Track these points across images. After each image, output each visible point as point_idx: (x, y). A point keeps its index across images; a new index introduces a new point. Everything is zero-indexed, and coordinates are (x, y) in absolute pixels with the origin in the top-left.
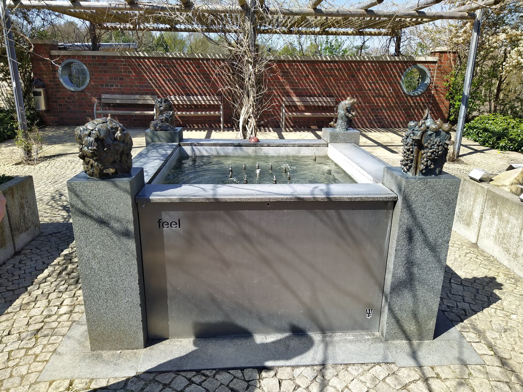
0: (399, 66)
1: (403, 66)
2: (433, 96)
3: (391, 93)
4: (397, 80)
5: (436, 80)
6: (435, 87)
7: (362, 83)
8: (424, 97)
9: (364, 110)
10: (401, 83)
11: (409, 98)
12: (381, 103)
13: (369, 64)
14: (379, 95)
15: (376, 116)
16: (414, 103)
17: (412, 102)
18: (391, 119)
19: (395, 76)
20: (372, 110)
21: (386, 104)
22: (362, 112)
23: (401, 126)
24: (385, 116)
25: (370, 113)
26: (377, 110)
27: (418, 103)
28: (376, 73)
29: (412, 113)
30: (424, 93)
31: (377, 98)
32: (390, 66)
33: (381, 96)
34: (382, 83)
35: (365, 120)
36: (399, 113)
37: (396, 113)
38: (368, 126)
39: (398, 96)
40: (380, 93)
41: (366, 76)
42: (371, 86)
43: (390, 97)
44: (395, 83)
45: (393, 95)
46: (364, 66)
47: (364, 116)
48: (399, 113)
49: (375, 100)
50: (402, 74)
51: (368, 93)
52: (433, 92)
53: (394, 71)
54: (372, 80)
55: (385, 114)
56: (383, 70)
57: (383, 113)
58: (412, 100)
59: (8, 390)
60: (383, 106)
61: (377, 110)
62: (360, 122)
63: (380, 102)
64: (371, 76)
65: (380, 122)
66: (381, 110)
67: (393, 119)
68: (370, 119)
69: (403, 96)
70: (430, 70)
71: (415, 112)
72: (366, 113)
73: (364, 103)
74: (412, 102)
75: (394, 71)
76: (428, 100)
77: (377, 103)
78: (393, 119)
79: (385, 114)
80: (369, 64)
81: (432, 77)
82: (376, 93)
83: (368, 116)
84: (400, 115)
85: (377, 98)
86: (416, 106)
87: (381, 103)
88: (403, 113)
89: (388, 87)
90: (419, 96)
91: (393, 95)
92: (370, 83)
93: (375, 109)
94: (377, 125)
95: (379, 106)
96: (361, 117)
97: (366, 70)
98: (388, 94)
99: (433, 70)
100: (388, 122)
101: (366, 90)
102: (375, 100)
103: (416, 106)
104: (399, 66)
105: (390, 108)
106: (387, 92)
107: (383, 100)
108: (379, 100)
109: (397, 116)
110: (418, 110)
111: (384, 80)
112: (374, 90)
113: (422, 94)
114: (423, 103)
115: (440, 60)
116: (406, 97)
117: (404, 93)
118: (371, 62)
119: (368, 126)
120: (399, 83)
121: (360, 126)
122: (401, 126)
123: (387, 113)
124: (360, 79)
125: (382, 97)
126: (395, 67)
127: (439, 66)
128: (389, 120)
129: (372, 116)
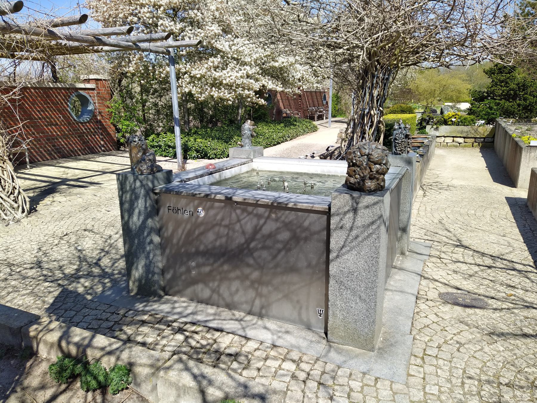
0: (62, 93)
1: (66, 92)
2: (100, 122)
3: (62, 120)
4: (64, 106)
5: (99, 106)
6: (100, 113)
7: (29, 111)
8: (92, 123)
9: (40, 140)
10: (69, 110)
11: (80, 124)
12: (56, 132)
13: (33, 91)
14: (51, 124)
15: (54, 146)
16: (86, 129)
17: (83, 128)
18: (69, 148)
19: (62, 104)
20: (48, 140)
21: (60, 132)
22: (38, 144)
23: (80, 153)
24: (62, 145)
25: (47, 144)
26: (53, 139)
27: (89, 129)
28: (42, 100)
29: (86, 139)
30: (92, 119)
31: (49, 127)
32: (54, 93)
33: (53, 124)
34: (51, 111)
35: (44, 153)
36: (75, 140)
37: (72, 141)
38: (49, 158)
39: (69, 124)
40: (51, 121)
41: (33, 104)
42: (41, 114)
43: (62, 124)
44: (63, 110)
45: (65, 123)
46: (28, 93)
47: (41, 147)
48: (75, 140)
49: (49, 129)
50: (68, 101)
51: (39, 122)
52: (99, 118)
53: (59, 97)
54: (40, 107)
55: (63, 143)
56: (48, 96)
57: (60, 142)
58: (83, 126)
59: (534, 44)
60: (58, 135)
61: (53, 139)
62: (38, 155)
63: (54, 131)
64: (37, 104)
65: (59, 152)
66: (57, 139)
67: (71, 148)
68: (48, 150)
69: (73, 123)
70: (91, 96)
71: (89, 138)
72: (43, 144)
73: (38, 133)
74: (83, 128)
75: (59, 97)
76: (97, 126)
77: (51, 132)
78: (71, 148)
79: (63, 143)
80: (33, 91)
81: (95, 103)
82: (47, 122)
83: (46, 147)
84: (77, 142)
85: (49, 127)
86: (88, 132)
87: (56, 132)
88: (78, 140)
89: (58, 114)
90: (88, 122)
91: (65, 123)
92: (38, 111)
93: (51, 139)
94: (57, 155)
95: (54, 135)
96: (38, 149)
97: (31, 97)
98: (60, 122)
99: (94, 97)
100: (67, 151)
101: (36, 119)
102: (49, 129)
103: (88, 132)
104: (62, 93)
105: (65, 136)
106: (58, 120)
107: (57, 128)
108: (53, 129)
109: (74, 144)
110: (91, 136)
111: (52, 108)
112: (45, 119)
113: (90, 120)
114: (93, 129)
115: (97, 87)
116: (77, 124)
117: (75, 120)
118: (35, 88)
119: (49, 158)
120: (67, 110)
121: (40, 159)
122: (80, 153)
123: (64, 142)
124: (26, 107)
125: (55, 125)
126: (59, 94)
127: (98, 93)
128: (68, 149)
129: (50, 147)
